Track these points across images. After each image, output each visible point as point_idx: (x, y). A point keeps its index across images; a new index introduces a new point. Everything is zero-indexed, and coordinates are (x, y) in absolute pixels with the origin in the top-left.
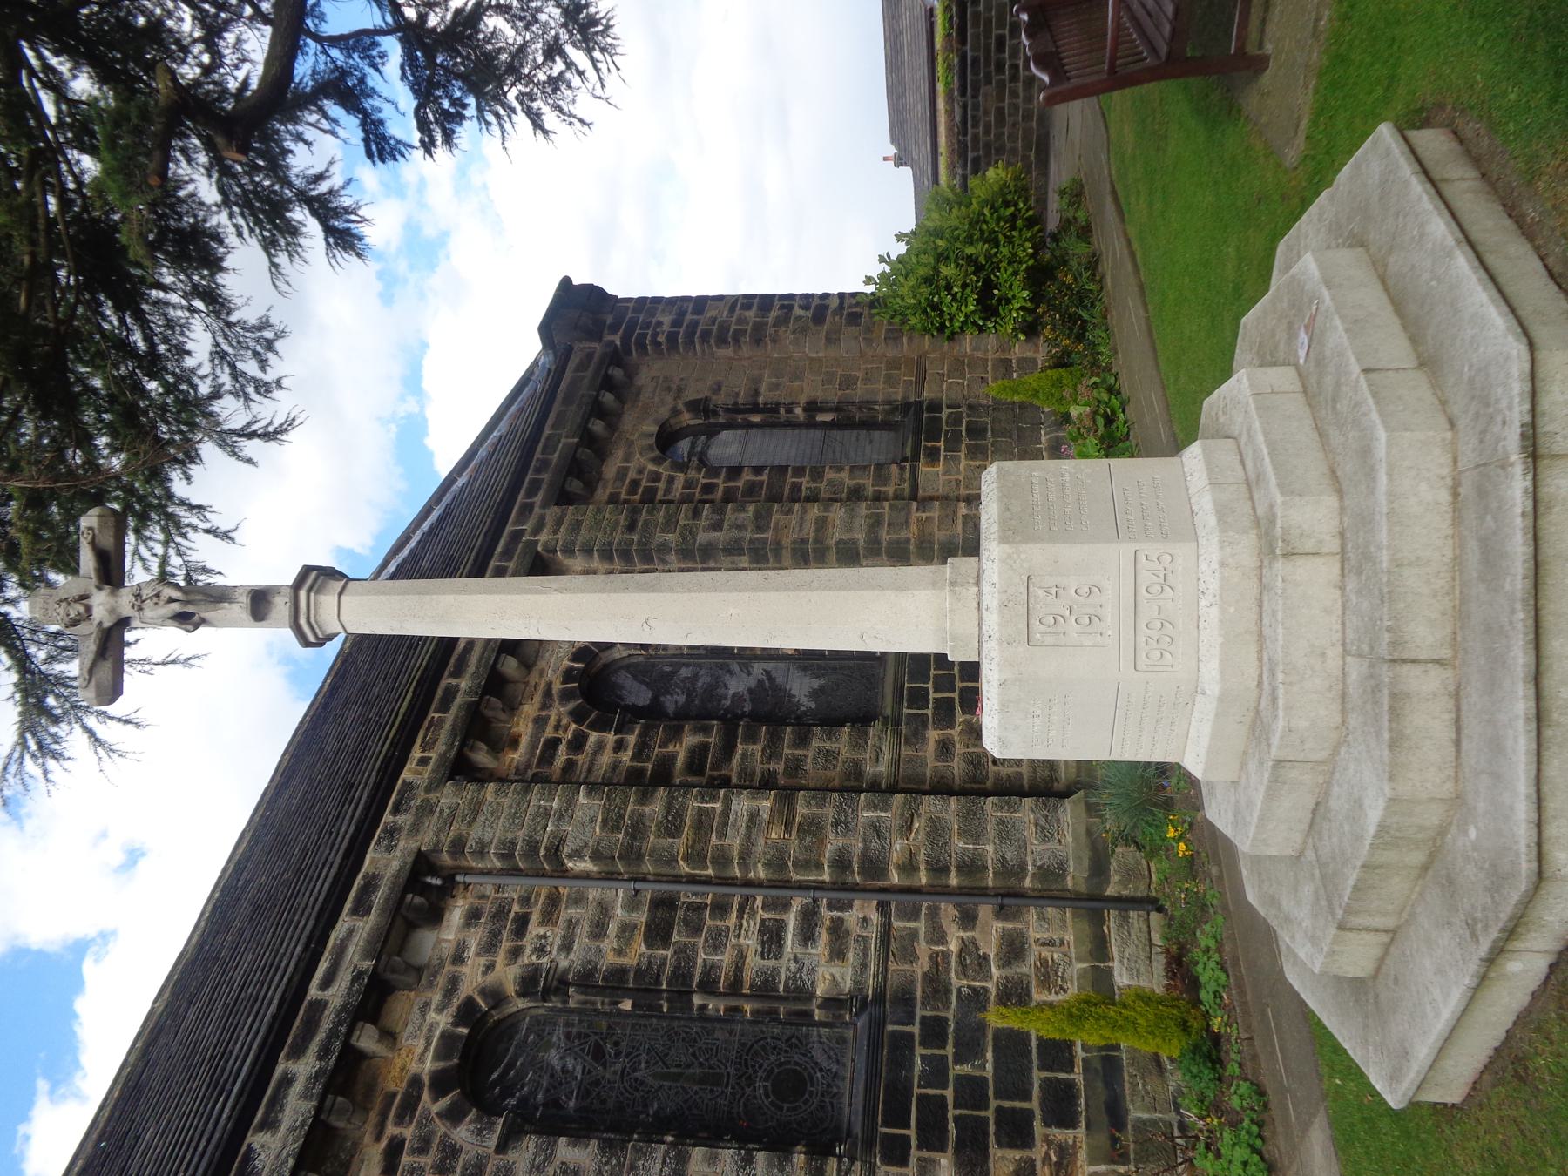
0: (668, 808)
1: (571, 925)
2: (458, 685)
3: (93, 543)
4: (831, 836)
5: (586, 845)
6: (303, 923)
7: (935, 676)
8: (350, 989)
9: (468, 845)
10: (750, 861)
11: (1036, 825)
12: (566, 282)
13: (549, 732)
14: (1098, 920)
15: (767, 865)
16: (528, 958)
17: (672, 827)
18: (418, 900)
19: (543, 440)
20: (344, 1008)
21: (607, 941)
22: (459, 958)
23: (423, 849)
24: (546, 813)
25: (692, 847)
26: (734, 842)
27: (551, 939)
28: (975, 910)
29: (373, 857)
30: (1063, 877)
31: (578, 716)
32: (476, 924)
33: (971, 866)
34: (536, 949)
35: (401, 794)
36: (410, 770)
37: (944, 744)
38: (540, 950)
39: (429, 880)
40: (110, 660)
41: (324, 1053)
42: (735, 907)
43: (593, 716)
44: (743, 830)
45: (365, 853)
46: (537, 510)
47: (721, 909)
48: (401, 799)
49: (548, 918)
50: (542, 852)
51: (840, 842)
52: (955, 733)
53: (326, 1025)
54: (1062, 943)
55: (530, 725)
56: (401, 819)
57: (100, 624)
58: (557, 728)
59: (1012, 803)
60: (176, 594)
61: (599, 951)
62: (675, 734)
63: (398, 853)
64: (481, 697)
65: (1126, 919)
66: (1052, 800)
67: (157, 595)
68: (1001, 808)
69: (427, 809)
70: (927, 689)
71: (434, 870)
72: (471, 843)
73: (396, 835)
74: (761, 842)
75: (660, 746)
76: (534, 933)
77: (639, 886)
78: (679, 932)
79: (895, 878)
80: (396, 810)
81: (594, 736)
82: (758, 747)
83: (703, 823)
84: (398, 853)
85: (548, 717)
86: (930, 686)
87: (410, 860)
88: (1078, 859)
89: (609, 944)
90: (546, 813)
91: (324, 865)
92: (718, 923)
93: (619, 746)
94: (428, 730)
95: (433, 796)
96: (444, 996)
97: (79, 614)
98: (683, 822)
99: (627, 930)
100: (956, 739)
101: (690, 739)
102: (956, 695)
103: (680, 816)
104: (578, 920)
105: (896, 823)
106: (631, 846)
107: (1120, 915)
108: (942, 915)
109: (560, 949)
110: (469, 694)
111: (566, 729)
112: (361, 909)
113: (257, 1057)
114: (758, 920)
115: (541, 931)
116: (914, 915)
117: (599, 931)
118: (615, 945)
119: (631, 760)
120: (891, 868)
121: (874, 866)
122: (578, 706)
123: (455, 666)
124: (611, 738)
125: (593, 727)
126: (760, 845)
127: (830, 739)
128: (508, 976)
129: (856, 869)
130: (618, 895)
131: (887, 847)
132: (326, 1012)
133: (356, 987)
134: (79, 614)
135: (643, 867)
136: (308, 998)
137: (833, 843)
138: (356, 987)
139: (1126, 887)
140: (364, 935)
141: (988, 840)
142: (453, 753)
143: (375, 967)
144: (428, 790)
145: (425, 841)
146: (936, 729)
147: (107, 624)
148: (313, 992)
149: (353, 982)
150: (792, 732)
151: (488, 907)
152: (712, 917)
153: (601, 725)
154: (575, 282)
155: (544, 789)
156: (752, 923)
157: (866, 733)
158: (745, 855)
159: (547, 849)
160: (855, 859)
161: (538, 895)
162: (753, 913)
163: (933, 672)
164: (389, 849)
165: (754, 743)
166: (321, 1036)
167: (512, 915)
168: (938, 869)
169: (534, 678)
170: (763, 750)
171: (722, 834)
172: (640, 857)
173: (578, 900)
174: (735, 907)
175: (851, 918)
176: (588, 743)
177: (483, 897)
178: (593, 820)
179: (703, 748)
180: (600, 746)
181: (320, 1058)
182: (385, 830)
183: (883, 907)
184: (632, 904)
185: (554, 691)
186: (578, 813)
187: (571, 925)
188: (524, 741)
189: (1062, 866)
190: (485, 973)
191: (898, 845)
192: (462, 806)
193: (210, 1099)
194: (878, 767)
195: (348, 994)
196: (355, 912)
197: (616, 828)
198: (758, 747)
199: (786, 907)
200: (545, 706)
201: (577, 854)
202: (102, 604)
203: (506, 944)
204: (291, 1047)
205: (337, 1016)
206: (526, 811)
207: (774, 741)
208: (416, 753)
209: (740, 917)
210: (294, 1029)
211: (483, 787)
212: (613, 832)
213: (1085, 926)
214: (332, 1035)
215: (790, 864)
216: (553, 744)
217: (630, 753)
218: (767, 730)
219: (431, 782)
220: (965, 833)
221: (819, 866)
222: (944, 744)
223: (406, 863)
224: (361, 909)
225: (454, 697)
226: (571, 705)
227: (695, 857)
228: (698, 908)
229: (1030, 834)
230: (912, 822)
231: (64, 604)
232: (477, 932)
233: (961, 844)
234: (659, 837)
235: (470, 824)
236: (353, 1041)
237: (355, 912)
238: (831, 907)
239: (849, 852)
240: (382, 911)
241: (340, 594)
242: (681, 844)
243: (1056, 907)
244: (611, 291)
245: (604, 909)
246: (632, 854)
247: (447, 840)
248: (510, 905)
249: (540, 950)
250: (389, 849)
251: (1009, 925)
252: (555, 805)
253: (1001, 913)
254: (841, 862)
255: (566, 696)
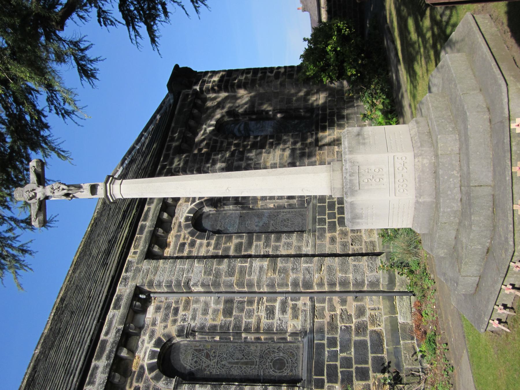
0: (229, 266)
1: (195, 310)
2: (146, 224)
3: (35, 171)
4: (291, 274)
5: (199, 281)
6: (95, 314)
7: (328, 213)
8: (115, 335)
9: (154, 283)
10: (261, 284)
11: (368, 266)
12: (177, 66)
13: (181, 241)
14: (392, 300)
15: (268, 285)
16: (179, 323)
17: (231, 273)
18: (138, 303)
19: (171, 129)
20: (114, 342)
21: (208, 316)
22: (154, 324)
23: (138, 285)
24: (183, 270)
25: (239, 280)
26: (254, 278)
27: (188, 316)
28: (346, 299)
29: (119, 288)
30: (378, 285)
31: (192, 234)
32: (159, 312)
33: (344, 283)
34: (182, 320)
35: (128, 265)
36: (130, 256)
37: (332, 238)
38: (184, 320)
39: (140, 296)
40: (43, 211)
41: (108, 358)
42: (256, 301)
43: (197, 234)
44: (258, 273)
45: (117, 287)
46: (171, 156)
47: (250, 302)
48: (128, 267)
49: (186, 308)
50: (182, 284)
51: (295, 276)
52: (337, 234)
53: (108, 348)
54: (379, 309)
55: (174, 238)
56: (128, 274)
57: (39, 199)
58: (184, 238)
59: (359, 259)
60: (65, 187)
61: (206, 319)
62: (230, 239)
63: (129, 287)
64: (155, 228)
65: (402, 299)
66: (374, 257)
67: (59, 188)
68: (355, 261)
69: (138, 270)
70: (325, 218)
71: (143, 292)
72: (155, 282)
73: (127, 281)
74: (265, 277)
75: (224, 244)
76: (181, 314)
77: (219, 295)
78: (235, 311)
79: (316, 289)
80: (126, 271)
81: (198, 241)
82: (262, 243)
83: (242, 271)
84: (129, 287)
85: (181, 235)
86: (326, 217)
87: (133, 289)
88: (384, 278)
89: (209, 317)
90: (183, 270)
91: (100, 293)
92: (250, 307)
93: (208, 245)
94: (136, 241)
95: (139, 266)
96: (150, 338)
97: (33, 195)
98: (235, 271)
99: (216, 311)
100: (337, 236)
101: (235, 241)
102: (336, 220)
103: (233, 268)
104: (197, 309)
105: (316, 268)
106: (216, 281)
107: (400, 298)
108: (334, 301)
109: (191, 319)
110: (150, 227)
111: (188, 239)
112: (117, 306)
113: (84, 360)
114: (265, 306)
115: (184, 313)
116: (324, 301)
117: (205, 312)
118: (212, 317)
119: (213, 249)
120: (314, 284)
121: (308, 284)
122: (192, 230)
123: (144, 217)
124: (205, 241)
125: (198, 237)
126: (264, 278)
127: (289, 238)
128: (173, 330)
129: (301, 286)
130: (211, 299)
131: (312, 277)
132: (108, 344)
133: (117, 335)
134: (33, 195)
135: (221, 288)
136: (101, 339)
137: (292, 276)
138: (117, 335)
139: (402, 287)
140: (119, 316)
141: (350, 272)
142: (146, 250)
143: (124, 327)
144: (138, 263)
145: (138, 282)
146: (329, 233)
147: (41, 199)
148: (102, 337)
149: (116, 333)
150: (274, 237)
151: (163, 305)
152: (248, 306)
153: (201, 237)
154: (180, 67)
155: (181, 261)
156: (262, 307)
157: (302, 236)
158: (259, 283)
159: (184, 283)
160: (301, 282)
161: (182, 300)
162: (263, 303)
163: (327, 212)
164: (125, 286)
165: (260, 241)
166: (107, 352)
167: (172, 308)
168: (332, 284)
169: (174, 220)
170: (263, 244)
171: (250, 275)
172: (219, 285)
173: (197, 301)
174: (256, 301)
175: (300, 303)
176: (197, 244)
177: (161, 302)
178: (201, 272)
179: (241, 244)
180: (201, 245)
181: (107, 360)
182: (123, 279)
183: (312, 299)
184: (217, 302)
185: (182, 225)
186: (195, 270)
187: (195, 310)
188: (172, 244)
189: (378, 281)
190: (164, 329)
191: (316, 276)
192: (151, 269)
193: (66, 377)
194: (308, 250)
195: (115, 337)
196: (114, 308)
197: (210, 274)
198: (262, 243)
199: (275, 300)
200: (179, 231)
201: (195, 285)
202: (40, 193)
203: (171, 318)
204: (96, 356)
205: (112, 345)
206: (175, 270)
207: (268, 240)
208: (132, 250)
209: (258, 304)
210: (97, 350)
211: (158, 261)
212: (208, 276)
213: (388, 303)
214: (111, 352)
215: (276, 285)
216: (183, 245)
217: (212, 247)
218: (265, 236)
219: (138, 261)
220: (341, 270)
221: (287, 285)
222: (332, 238)
223: (132, 290)
224: (117, 306)
225: (145, 229)
226: (189, 230)
227: (240, 284)
228: (242, 302)
229: (366, 269)
230: (321, 267)
231: (28, 192)
232: (160, 315)
233: (340, 275)
234: (226, 277)
235: (154, 275)
236: (118, 354)
237: (114, 308)
238: (292, 300)
239: (298, 280)
240: (125, 307)
241: (121, 184)
242: (234, 279)
243: (376, 296)
244: (194, 69)
245: (207, 304)
246: (216, 284)
247: (146, 281)
248: (172, 304)
249: (184, 320)
250: (125, 286)
251: (359, 303)
252: (186, 267)
253: (356, 299)
254: (295, 284)
255: (187, 226)
